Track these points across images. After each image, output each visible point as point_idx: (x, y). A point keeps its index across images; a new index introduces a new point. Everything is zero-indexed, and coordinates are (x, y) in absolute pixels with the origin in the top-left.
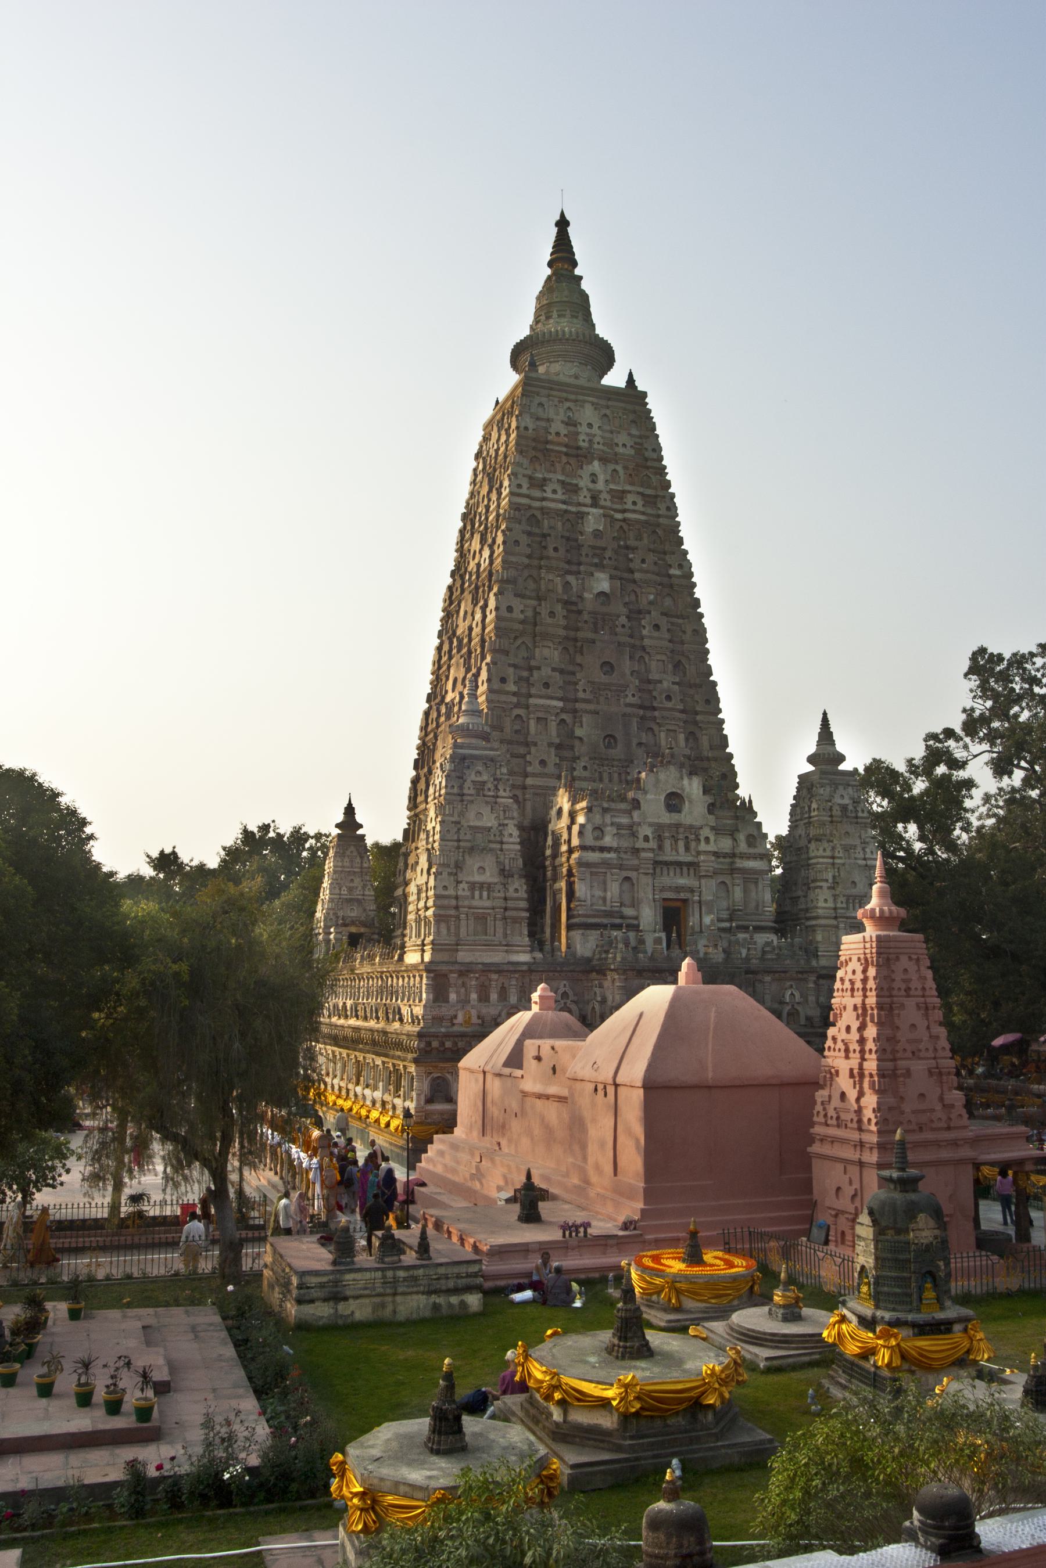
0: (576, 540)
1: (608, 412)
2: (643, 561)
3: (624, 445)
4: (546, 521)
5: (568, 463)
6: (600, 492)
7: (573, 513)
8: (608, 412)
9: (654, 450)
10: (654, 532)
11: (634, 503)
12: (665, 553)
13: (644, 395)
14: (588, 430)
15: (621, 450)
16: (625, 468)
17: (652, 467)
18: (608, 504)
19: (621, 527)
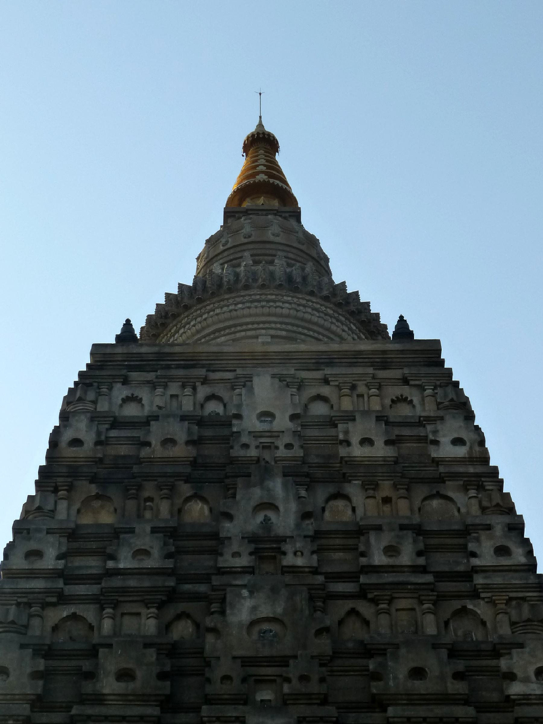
0: (199, 652)
1: (325, 391)
2: (418, 673)
3: (366, 441)
4: (107, 625)
5: (197, 496)
6: (283, 539)
7: (196, 597)
8: (325, 391)
9: (458, 442)
10: (463, 611)
11: (391, 550)
12: (496, 652)
13: (434, 347)
14: (259, 426)
15: (358, 451)
16: (370, 486)
17: (454, 476)
18: (300, 562)
19: (353, 612)
